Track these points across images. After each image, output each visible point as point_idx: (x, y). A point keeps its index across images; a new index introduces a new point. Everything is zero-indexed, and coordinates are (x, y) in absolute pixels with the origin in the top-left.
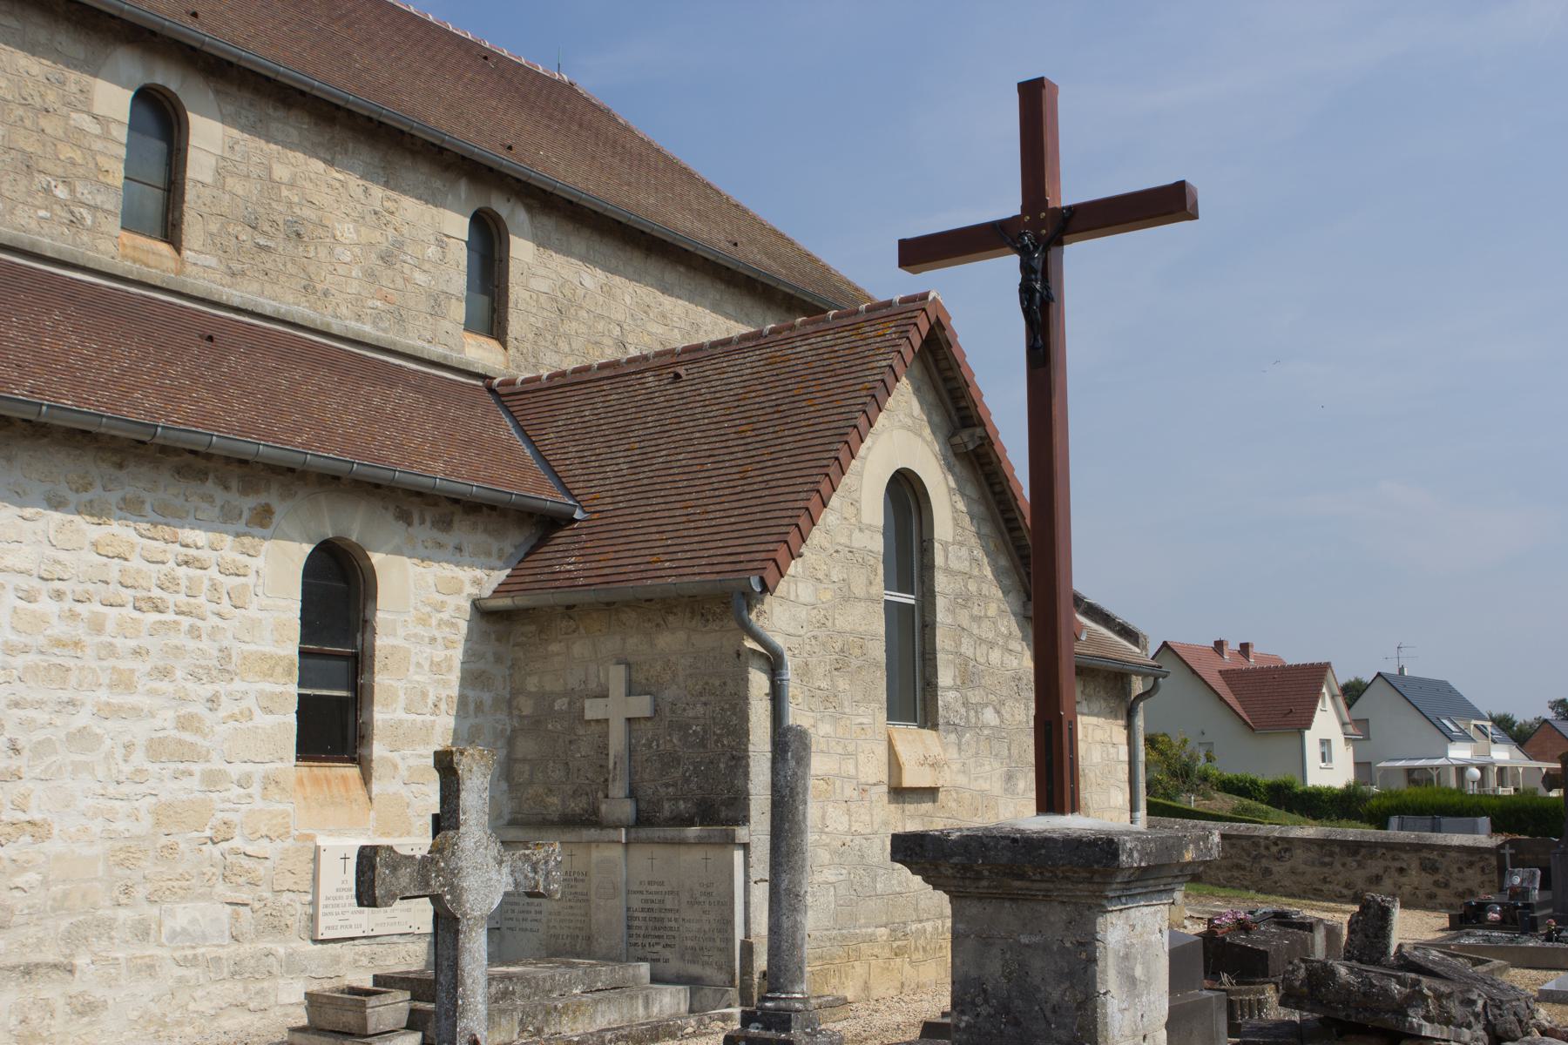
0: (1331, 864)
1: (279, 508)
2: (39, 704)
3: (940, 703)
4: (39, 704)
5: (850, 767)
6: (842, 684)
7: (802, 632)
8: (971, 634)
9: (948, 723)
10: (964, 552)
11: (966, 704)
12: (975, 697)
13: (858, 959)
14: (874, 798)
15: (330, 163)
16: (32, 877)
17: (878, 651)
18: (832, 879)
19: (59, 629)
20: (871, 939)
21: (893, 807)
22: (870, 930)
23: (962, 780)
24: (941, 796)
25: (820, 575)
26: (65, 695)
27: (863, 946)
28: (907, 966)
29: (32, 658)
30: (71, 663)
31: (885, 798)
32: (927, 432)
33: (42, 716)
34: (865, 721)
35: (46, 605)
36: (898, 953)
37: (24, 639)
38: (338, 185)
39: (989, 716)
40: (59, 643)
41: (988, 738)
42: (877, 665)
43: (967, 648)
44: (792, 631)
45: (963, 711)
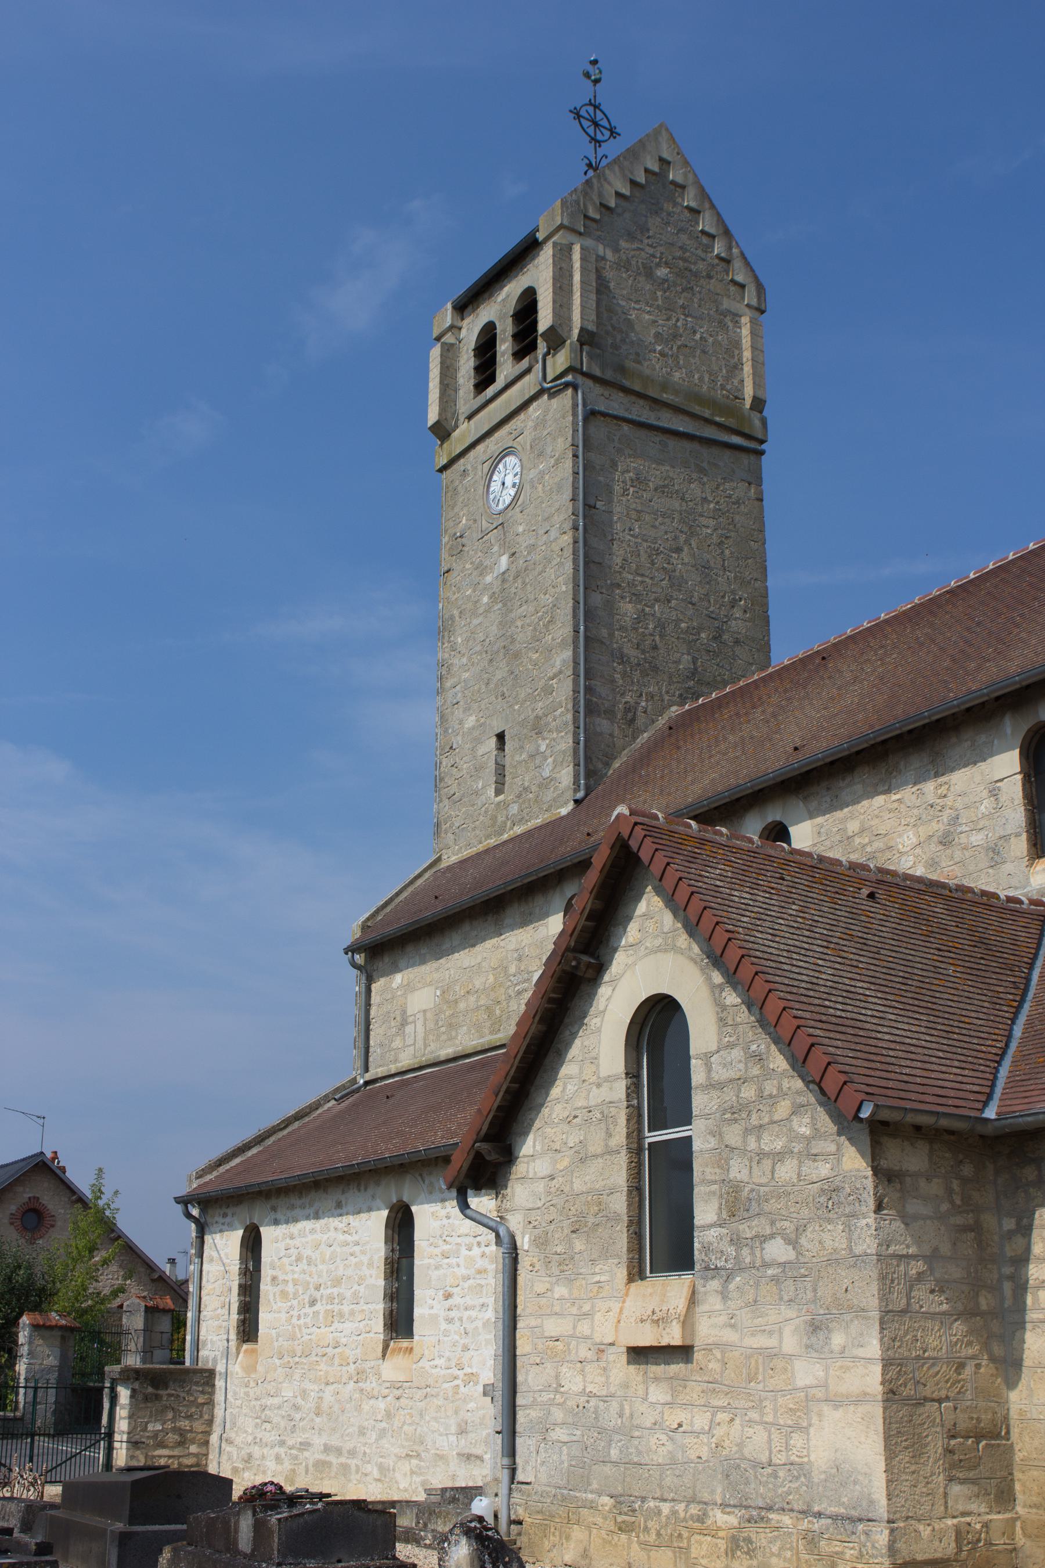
0: (327, 1449)
1: (343, 1198)
2: (473, 1308)
3: (697, 1245)
4: (473, 1308)
5: (584, 1328)
6: (579, 1245)
7: (540, 1204)
8: (744, 1151)
9: (707, 1268)
10: (737, 1053)
11: (736, 1241)
12: (747, 1230)
13: (578, 1523)
14: (611, 1358)
15: (888, 791)
16: (471, 1405)
17: (619, 1204)
18: (565, 1438)
19: (480, 1263)
20: (592, 1506)
21: (632, 1368)
22: (590, 1496)
23: (730, 1336)
24: (697, 1356)
25: (557, 1146)
26: (481, 1301)
27: (585, 1512)
28: (635, 1546)
29: (471, 1281)
30: (483, 1282)
31: (624, 1358)
32: (683, 940)
33: (473, 1313)
34: (603, 1279)
35: (476, 1251)
36: (624, 1528)
37: (468, 1272)
38: (896, 805)
39: (777, 1250)
40: (479, 1272)
41: (775, 1280)
42: (617, 1218)
43: (738, 1170)
44: (531, 1206)
45: (731, 1250)
